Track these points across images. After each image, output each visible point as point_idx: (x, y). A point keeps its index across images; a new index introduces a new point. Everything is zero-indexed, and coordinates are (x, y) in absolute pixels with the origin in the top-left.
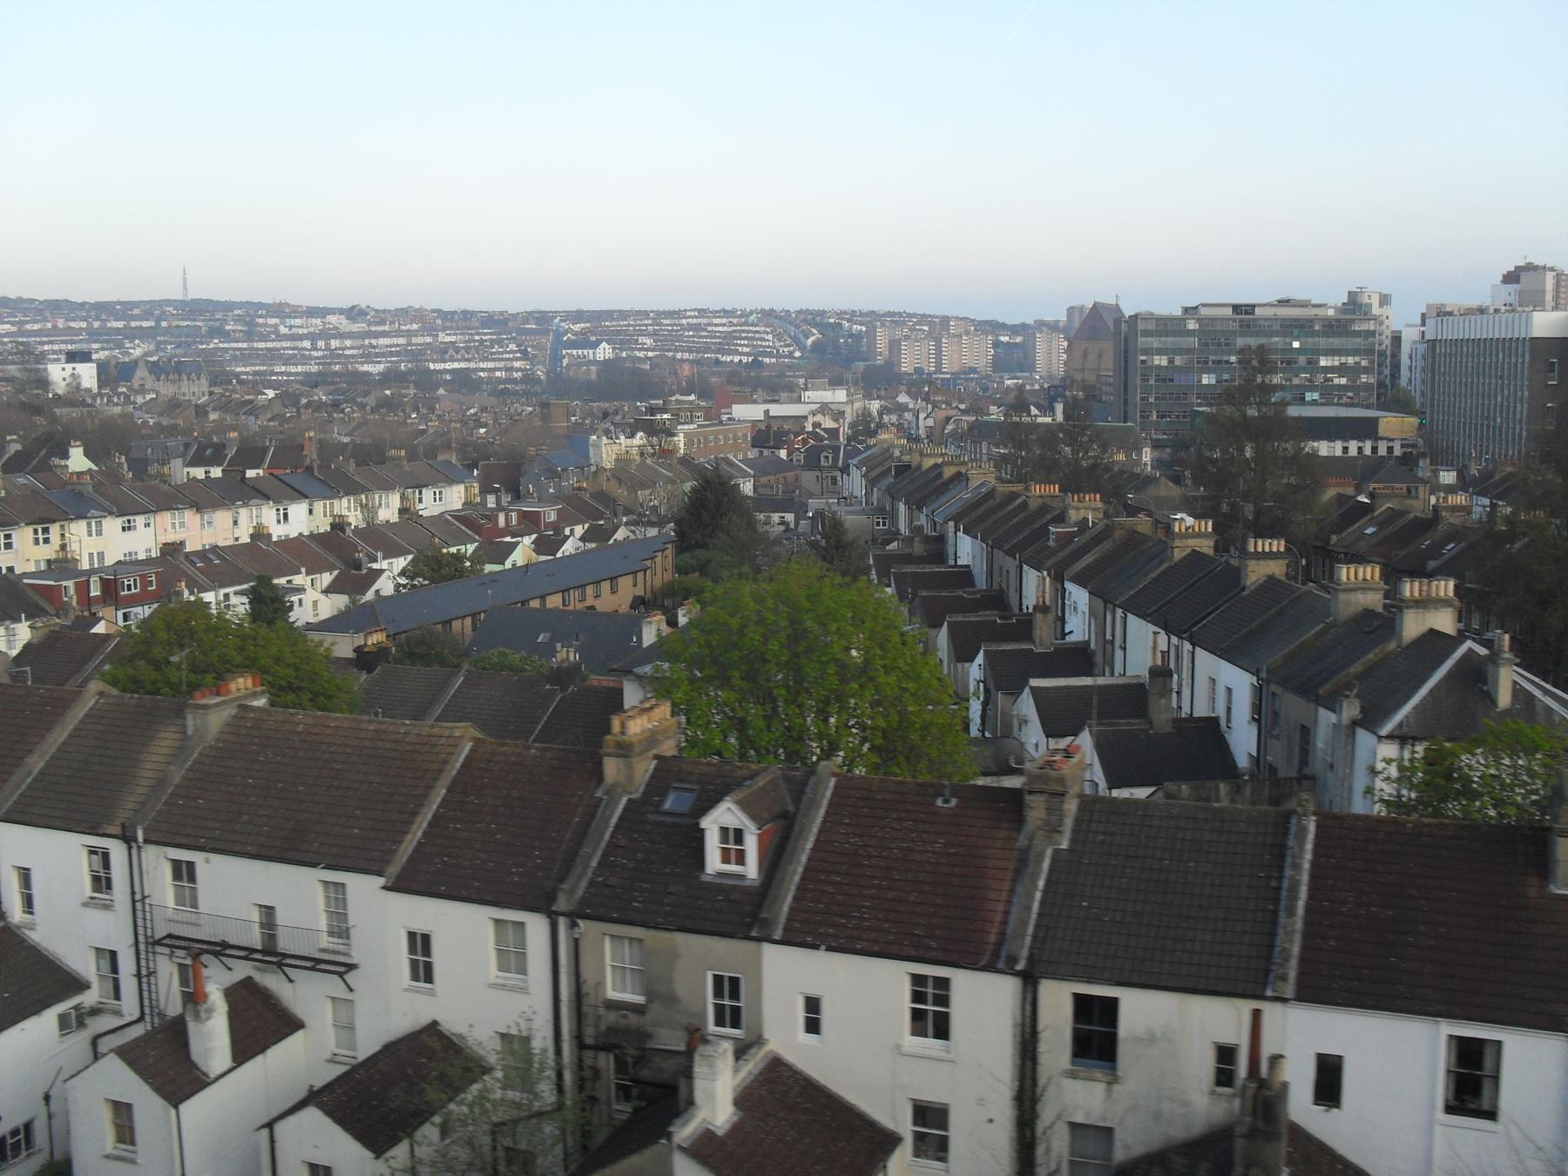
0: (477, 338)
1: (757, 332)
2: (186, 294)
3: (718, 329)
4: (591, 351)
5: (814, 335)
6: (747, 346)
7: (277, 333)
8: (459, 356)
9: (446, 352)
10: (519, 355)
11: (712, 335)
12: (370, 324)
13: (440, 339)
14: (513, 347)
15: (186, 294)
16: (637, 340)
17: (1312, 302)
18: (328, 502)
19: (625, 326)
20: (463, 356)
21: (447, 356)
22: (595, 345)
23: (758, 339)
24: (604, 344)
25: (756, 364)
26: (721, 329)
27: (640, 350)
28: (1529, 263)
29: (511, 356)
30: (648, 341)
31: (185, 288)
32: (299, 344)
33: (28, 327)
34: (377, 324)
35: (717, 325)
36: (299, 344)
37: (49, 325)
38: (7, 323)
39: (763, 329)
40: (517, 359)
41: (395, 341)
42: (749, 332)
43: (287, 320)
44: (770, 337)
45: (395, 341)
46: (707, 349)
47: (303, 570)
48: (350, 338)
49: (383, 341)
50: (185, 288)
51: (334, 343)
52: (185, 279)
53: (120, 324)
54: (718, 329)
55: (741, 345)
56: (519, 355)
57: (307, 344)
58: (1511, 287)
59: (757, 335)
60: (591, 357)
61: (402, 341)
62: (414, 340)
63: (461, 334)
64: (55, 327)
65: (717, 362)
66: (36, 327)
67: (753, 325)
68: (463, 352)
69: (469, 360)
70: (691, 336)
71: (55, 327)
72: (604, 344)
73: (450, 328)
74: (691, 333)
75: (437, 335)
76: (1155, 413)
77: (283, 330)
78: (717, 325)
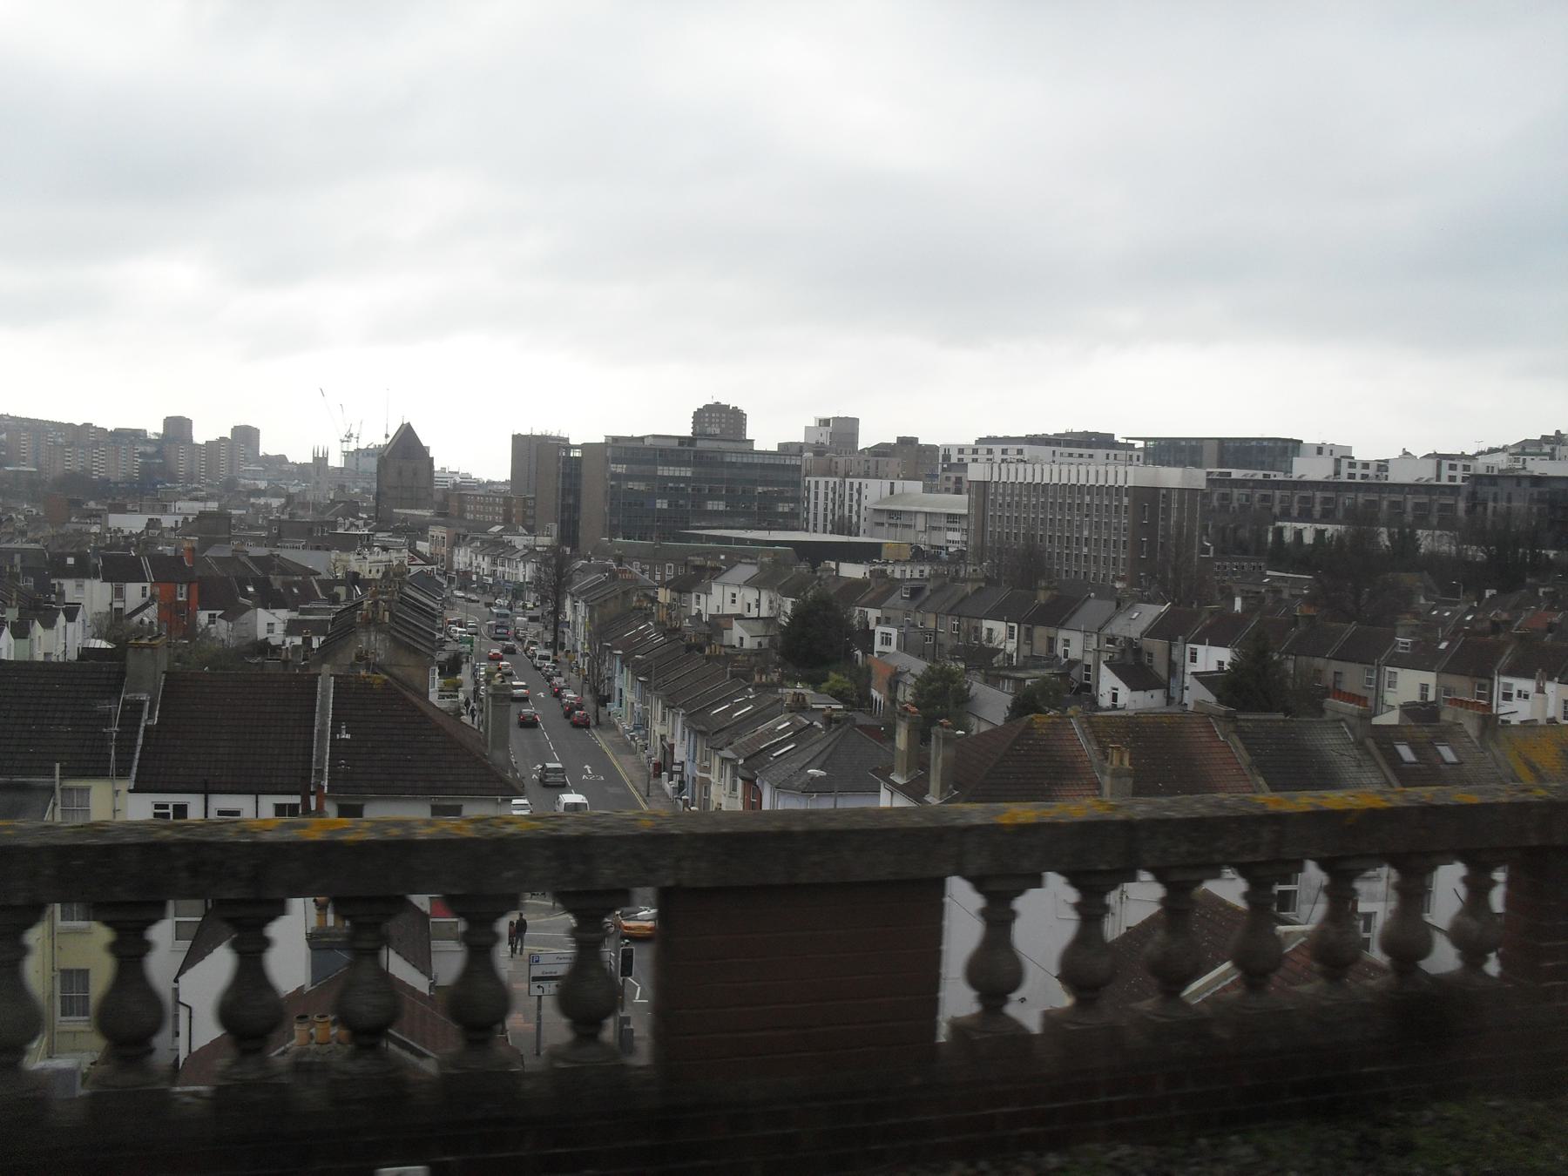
28: (718, 403)
58: (824, 430)
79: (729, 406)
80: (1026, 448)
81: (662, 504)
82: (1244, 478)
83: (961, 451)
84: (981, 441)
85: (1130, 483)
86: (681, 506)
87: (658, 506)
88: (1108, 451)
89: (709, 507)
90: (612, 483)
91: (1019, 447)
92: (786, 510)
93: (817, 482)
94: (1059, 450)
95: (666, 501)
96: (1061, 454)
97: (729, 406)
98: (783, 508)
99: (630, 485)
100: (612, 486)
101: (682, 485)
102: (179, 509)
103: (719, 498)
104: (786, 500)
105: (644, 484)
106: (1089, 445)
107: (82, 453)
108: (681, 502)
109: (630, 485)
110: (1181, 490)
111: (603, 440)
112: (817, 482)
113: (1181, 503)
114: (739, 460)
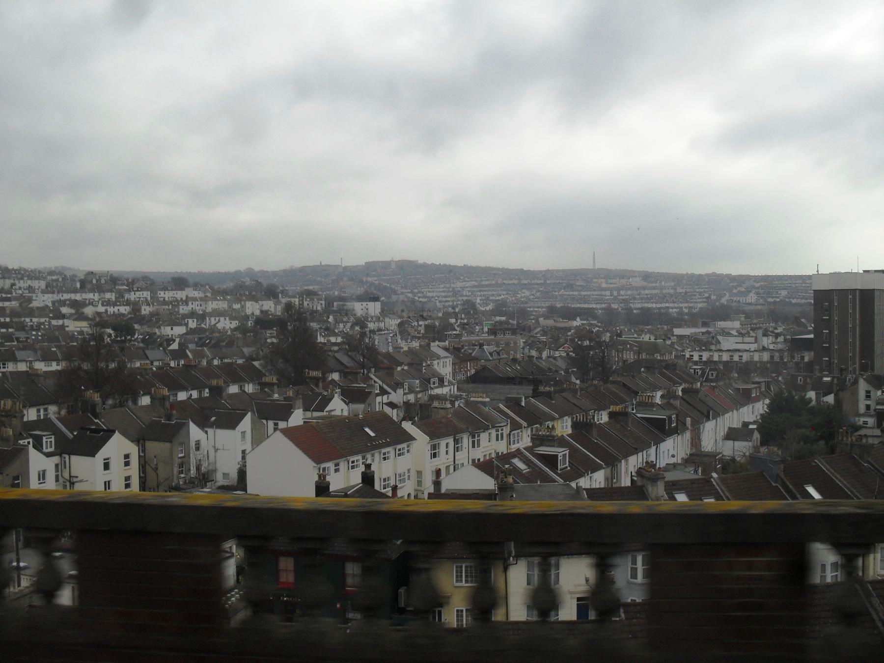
0: (697, 290)
2: (594, 265)
4: (744, 298)
13: (678, 291)
15: (594, 265)
16: (777, 292)
19: (787, 284)
29: (701, 300)
31: (594, 262)
32: (603, 293)
33: (483, 283)
34: (652, 282)
36: (603, 293)
37: (494, 282)
38: (474, 281)
43: (609, 280)
50: (594, 262)
52: (594, 258)
53: (526, 282)
56: (704, 300)
57: (608, 293)
60: (744, 301)
62: (664, 291)
63: (689, 288)
64: (497, 283)
66: (487, 283)
69: (674, 302)
71: (497, 283)
75: (676, 289)
77: (604, 285)
102: (720, 325)
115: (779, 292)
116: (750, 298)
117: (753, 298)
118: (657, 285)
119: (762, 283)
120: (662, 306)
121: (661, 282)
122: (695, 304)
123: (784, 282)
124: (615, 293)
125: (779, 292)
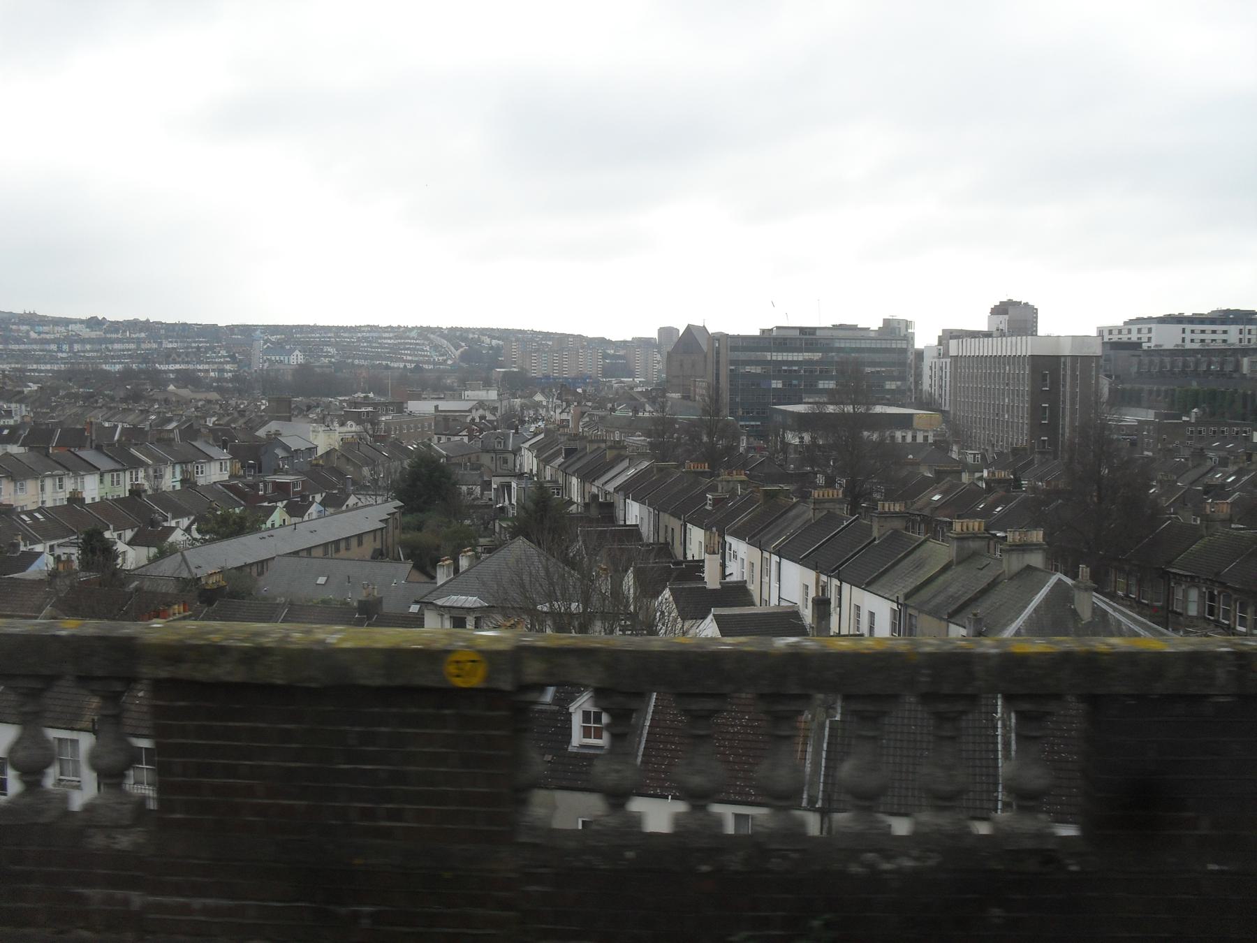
0: (194, 345)
1: (417, 344)
3: (386, 341)
4: (286, 358)
5: (462, 347)
6: (410, 355)
7: (28, 337)
8: (180, 359)
9: (170, 356)
10: (228, 359)
11: (381, 346)
12: (106, 332)
14: (223, 353)
16: (322, 349)
17: (859, 327)
18: (115, 474)
20: (183, 359)
21: (171, 359)
22: (290, 352)
23: (418, 350)
24: (297, 352)
25: (418, 369)
26: (389, 341)
27: (325, 357)
30: (332, 350)
32: (47, 347)
35: (385, 338)
36: (47, 347)
39: (422, 342)
40: (228, 363)
41: (127, 346)
42: (411, 344)
43: (37, 327)
44: (428, 348)
45: (127, 346)
46: (379, 356)
47: (111, 527)
48: (89, 343)
49: (117, 346)
51: (77, 347)
54: (386, 341)
55: (406, 355)
56: (228, 359)
57: (53, 347)
59: (418, 347)
61: (132, 346)
62: (143, 346)
65: (387, 367)
67: (413, 338)
68: (183, 356)
69: (188, 363)
70: (365, 347)
72: (297, 352)
73: (172, 337)
74: (365, 344)
76: (740, 409)
77: (33, 335)
78: (385, 338)
79: (1021, 302)
80: (1153, 326)
81: (777, 384)
82: (1176, 348)
83: (1110, 332)
84: (1131, 322)
85: (1029, 354)
86: (795, 385)
87: (774, 386)
88: (1242, 327)
89: (888, 387)
90: (733, 367)
91: (1149, 326)
92: (894, 387)
93: (946, 362)
94: (1189, 327)
95: (781, 381)
96: (1193, 332)
97: (1021, 302)
98: (891, 385)
99: (748, 369)
100: (731, 370)
101: (796, 368)
103: (831, 378)
104: (893, 379)
105: (760, 367)
106: (1223, 322)
107: (545, 357)
108: (795, 382)
109: (748, 369)
110: (1074, 358)
111: (757, 333)
112: (946, 362)
113: (1073, 370)
114: (848, 345)
115: (325, 350)
116: (295, 357)
117: (299, 359)
118: (119, 336)
119: (278, 337)
120: (170, 368)
121: (124, 332)
122: (221, 365)
123: (310, 336)
124: (66, 347)
125: (325, 350)
